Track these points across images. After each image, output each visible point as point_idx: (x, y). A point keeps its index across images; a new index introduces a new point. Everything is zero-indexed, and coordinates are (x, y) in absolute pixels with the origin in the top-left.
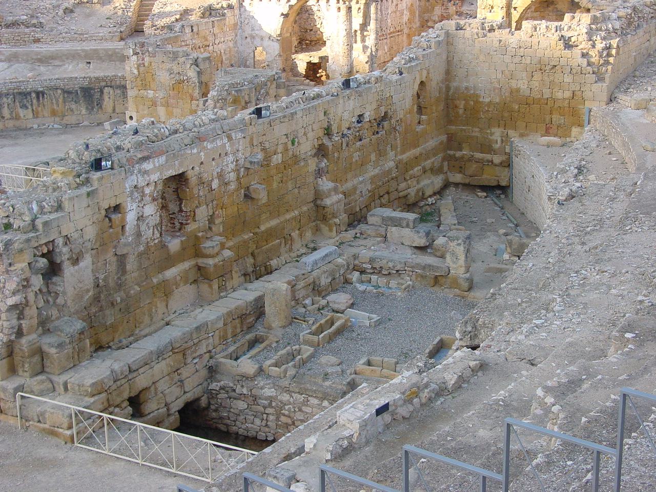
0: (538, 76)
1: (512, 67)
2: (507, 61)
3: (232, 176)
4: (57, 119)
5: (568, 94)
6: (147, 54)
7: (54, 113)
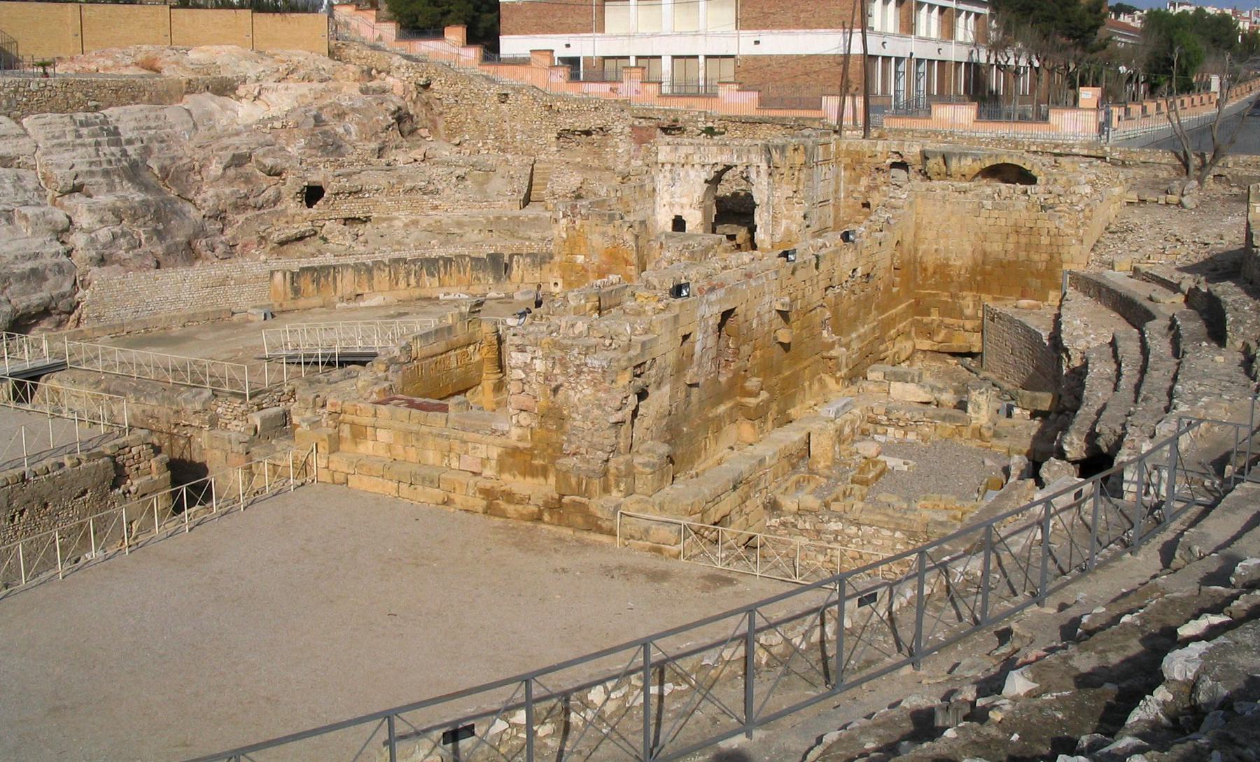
0: (1013, 238)
1: (985, 229)
4: (464, 289)
5: (1045, 257)
6: (579, 216)
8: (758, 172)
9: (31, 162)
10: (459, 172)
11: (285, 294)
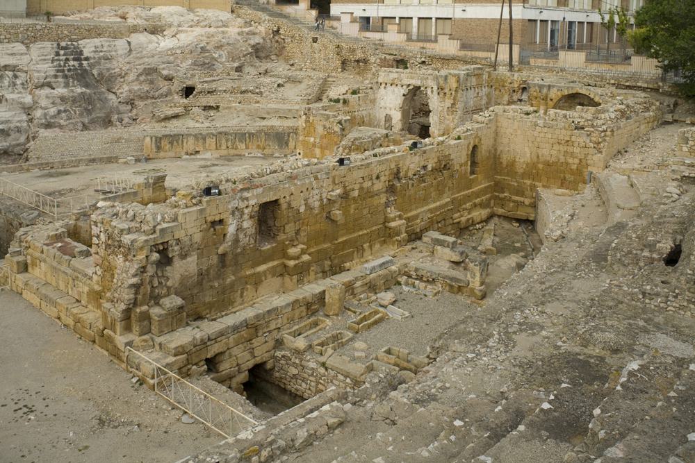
2: (535, 135)
3: (317, 204)
4: (261, 151)
5: (577, 161)
7: (258, 147)
8: (432, 92)
9: (26, 69)
10: (280, 81)
11: (151, 149)
